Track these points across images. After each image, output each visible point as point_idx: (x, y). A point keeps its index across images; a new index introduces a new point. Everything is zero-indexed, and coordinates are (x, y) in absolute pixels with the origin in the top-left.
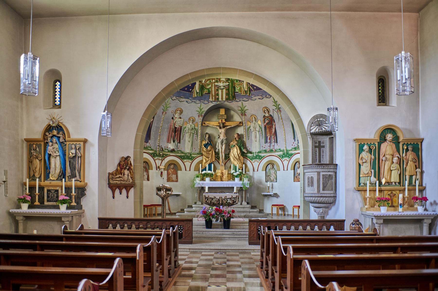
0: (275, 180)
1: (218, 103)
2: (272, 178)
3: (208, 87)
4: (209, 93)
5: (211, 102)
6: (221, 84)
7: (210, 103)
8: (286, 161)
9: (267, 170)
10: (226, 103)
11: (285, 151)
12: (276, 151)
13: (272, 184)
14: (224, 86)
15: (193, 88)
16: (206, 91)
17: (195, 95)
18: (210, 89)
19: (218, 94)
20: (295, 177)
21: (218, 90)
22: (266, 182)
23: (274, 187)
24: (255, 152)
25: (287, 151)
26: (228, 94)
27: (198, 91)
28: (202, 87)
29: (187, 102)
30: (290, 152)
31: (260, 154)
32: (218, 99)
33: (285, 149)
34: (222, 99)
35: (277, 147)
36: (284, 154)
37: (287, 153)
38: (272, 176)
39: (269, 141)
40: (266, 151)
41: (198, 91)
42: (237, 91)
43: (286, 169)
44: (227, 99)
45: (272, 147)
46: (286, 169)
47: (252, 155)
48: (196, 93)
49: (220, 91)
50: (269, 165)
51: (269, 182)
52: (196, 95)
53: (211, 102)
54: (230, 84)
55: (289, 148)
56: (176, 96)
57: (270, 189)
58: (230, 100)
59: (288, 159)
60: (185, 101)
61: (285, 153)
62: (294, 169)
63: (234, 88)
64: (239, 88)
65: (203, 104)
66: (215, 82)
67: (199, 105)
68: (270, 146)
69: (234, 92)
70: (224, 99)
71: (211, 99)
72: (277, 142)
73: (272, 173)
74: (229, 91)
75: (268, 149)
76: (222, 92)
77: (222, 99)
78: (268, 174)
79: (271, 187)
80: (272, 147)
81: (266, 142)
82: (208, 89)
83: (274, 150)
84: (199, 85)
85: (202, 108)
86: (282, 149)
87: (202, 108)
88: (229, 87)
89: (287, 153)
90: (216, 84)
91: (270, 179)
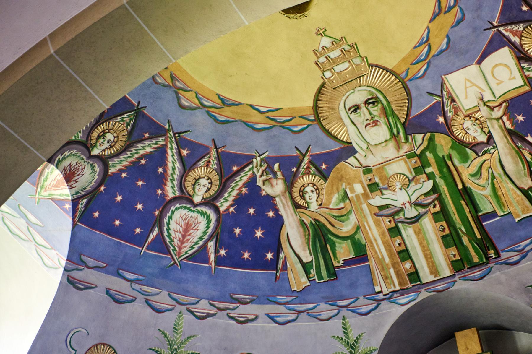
1: (424, 295)
3: (346, 228)
4: (361, 256)
5: (390, 297)
6: (399, 197)
7: (385, 305)
10: (461, 286)
14: (417, 204)
15: (278, 249)
16: (344, 252)
17: (298, 279)
18: (360, 236)
19: (405, 254)
21: (395, 231)
26: (451, 239)
27: (307, 257)
28: (320, 236)
29: (272, 318)
32: (414, 276)
34: (434, 271)
41: (307, 257)
42: (486, 208)
44: (460, 266)
48: (299, 266)
49: (409, 233)
52: (304, 279)
53: (390, 297)
54: (441, 182)
56: (211, 299)
58: (473, 266)
60: (263, 319)
63: (466, 194)
64: (488, 191)
65: (353, 320)
66: (366, 196)
67: (337, 323)
69: (479, 220)
70: (447, 272)
71: (381, 286)
74: (450, 224)
76: (419, 233)
77: (434, 271)
82: (351, 238)
84: (302, 223)
85: (353, 336)
87: (353, 336)
88: (440, 199)
90: (377, 201)
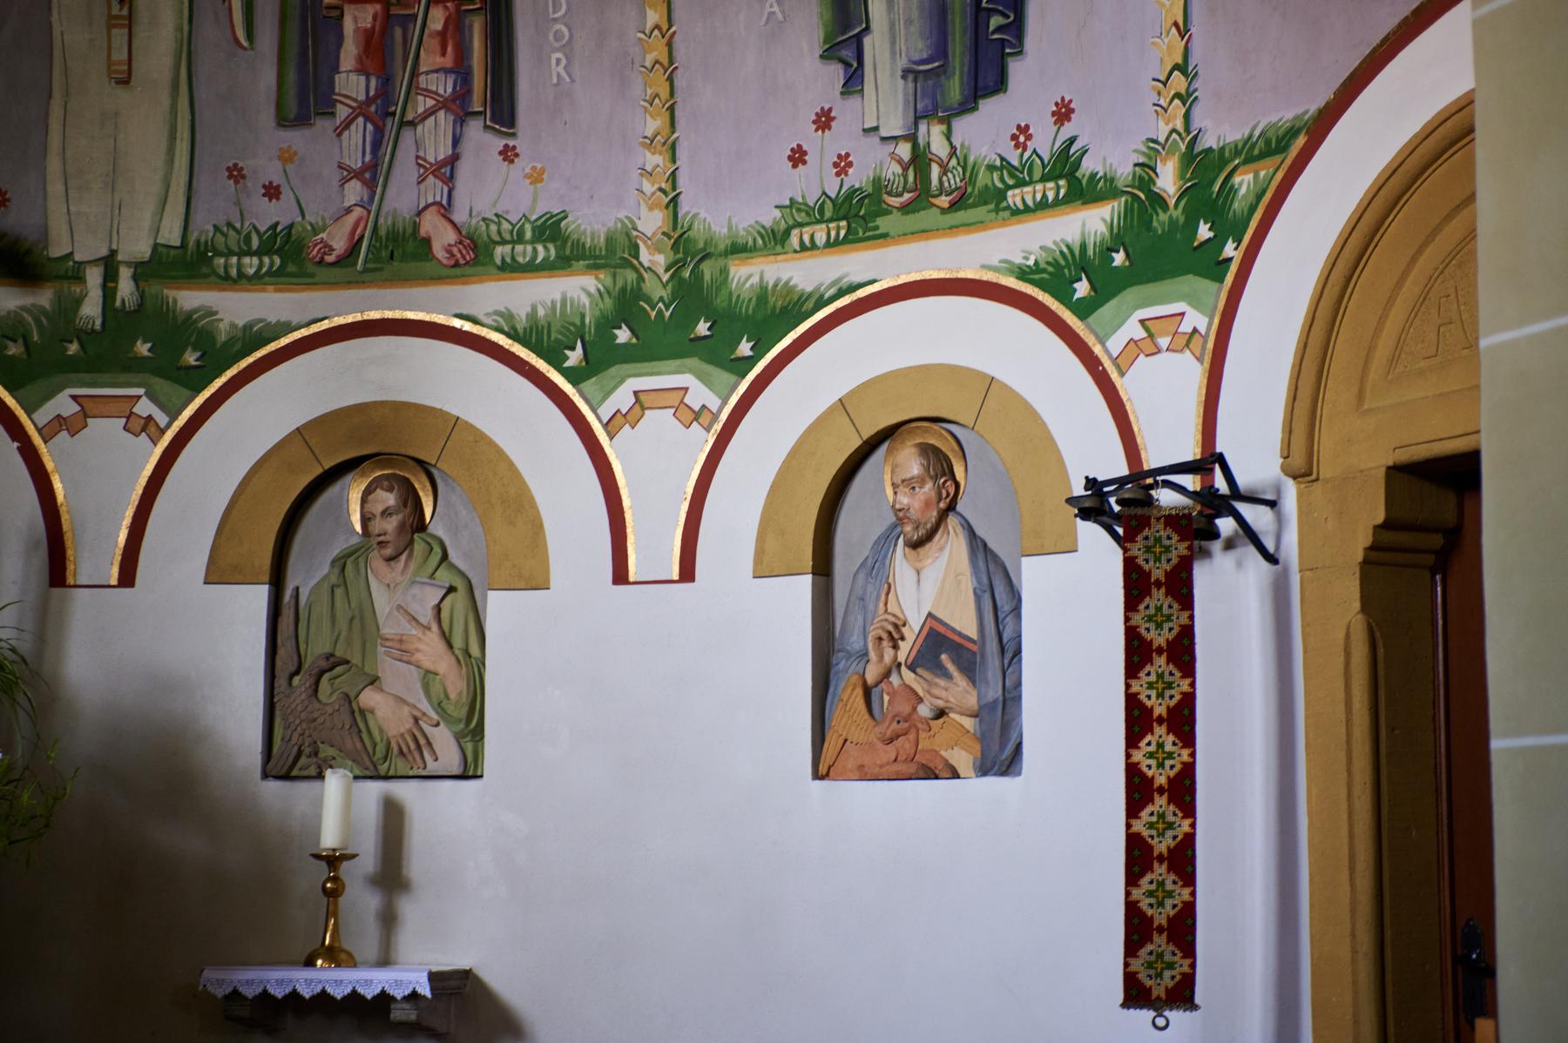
0: (444, 741)
2: (389, 707)
8: (659, 421)
9: (306, 576)
11: (654, 259)
12: (476, 256)
13: (393, 814)
20: (848, 699)
22: (290, 758)
23: (418, 862)
24: (89, 248)
25: (685, 247)
30: (747, 275)
31: (189, 299)
33: (652, 222)
35: (493, 188)
36: (627, 305)
37: (692, 294)
38: (398, 677)
39: (352, 85)
40: (291, 257)
43: (652, 548)
45: (404, 195)
46: (652, 548)
47: (44, 298)
50: (353, 491)
51: (334, 784)
55: (719, 214)
57: (361, 901)
59: (700, 395)
61: (656, 289)
62: (823, 567)
68: (372, 174)
72: (503, 114)
73: (391, 626)
75: (331, 210)
78: (318, 645)
79: (368, 859)
80: (404, 195)
81: (306, 101)
83: (442, 237)
86: (591, 221)
89: (692, 294)
91: (358, 717)
